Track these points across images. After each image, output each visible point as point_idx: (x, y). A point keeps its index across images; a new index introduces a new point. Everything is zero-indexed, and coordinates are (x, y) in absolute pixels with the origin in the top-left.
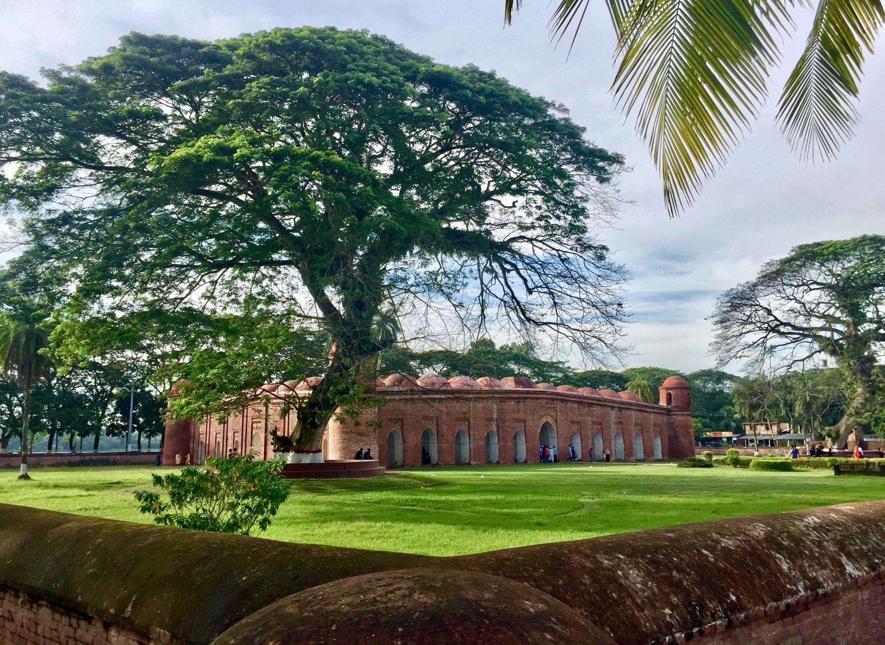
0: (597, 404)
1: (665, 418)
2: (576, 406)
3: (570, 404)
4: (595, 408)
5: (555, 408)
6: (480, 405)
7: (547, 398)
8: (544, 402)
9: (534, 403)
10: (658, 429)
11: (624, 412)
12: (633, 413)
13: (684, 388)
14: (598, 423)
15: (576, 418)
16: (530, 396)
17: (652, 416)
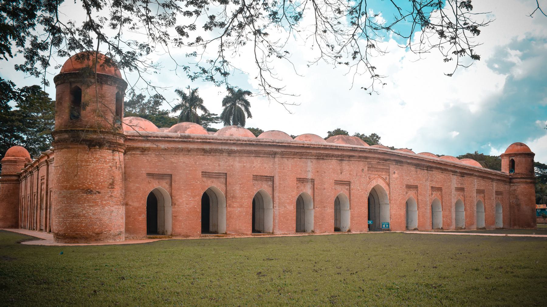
5: (388, 171)
7: (379, 159)
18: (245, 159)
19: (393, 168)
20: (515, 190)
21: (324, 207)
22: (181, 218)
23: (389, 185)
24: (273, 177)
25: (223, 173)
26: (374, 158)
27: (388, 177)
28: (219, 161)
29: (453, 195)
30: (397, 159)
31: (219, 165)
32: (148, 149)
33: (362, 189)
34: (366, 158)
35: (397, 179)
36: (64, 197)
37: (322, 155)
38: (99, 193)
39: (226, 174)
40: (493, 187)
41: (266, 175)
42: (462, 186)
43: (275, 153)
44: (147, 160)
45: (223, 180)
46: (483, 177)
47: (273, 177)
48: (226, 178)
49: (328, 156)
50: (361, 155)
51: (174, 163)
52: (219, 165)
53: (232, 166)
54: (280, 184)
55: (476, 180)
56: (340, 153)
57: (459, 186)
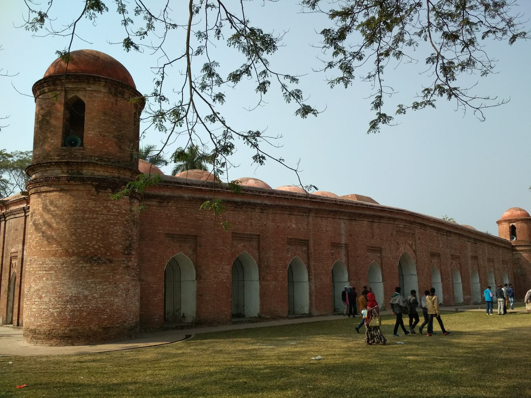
7: (406, 221)
21: (359, 279)
22: (207, 298)
23: (415, 252)
24: (308, 241)
25: (255, 235)
26: (402, 220)
27: (414, 242)
28: (251, 219)
31: (251, 225)
33: (392, 258)
36: (51, 269)
37: (355, 214)
38: (111, 261)
39: (259, 236)
41: (301, 238)
44: (167, 214)
45: (255, 244)
47: (308, 241)
48: (259, 242)
49: (360, 215)
51: (199, 220)
52: (251, 225)
53: (265, 225)
54: (315, 250)
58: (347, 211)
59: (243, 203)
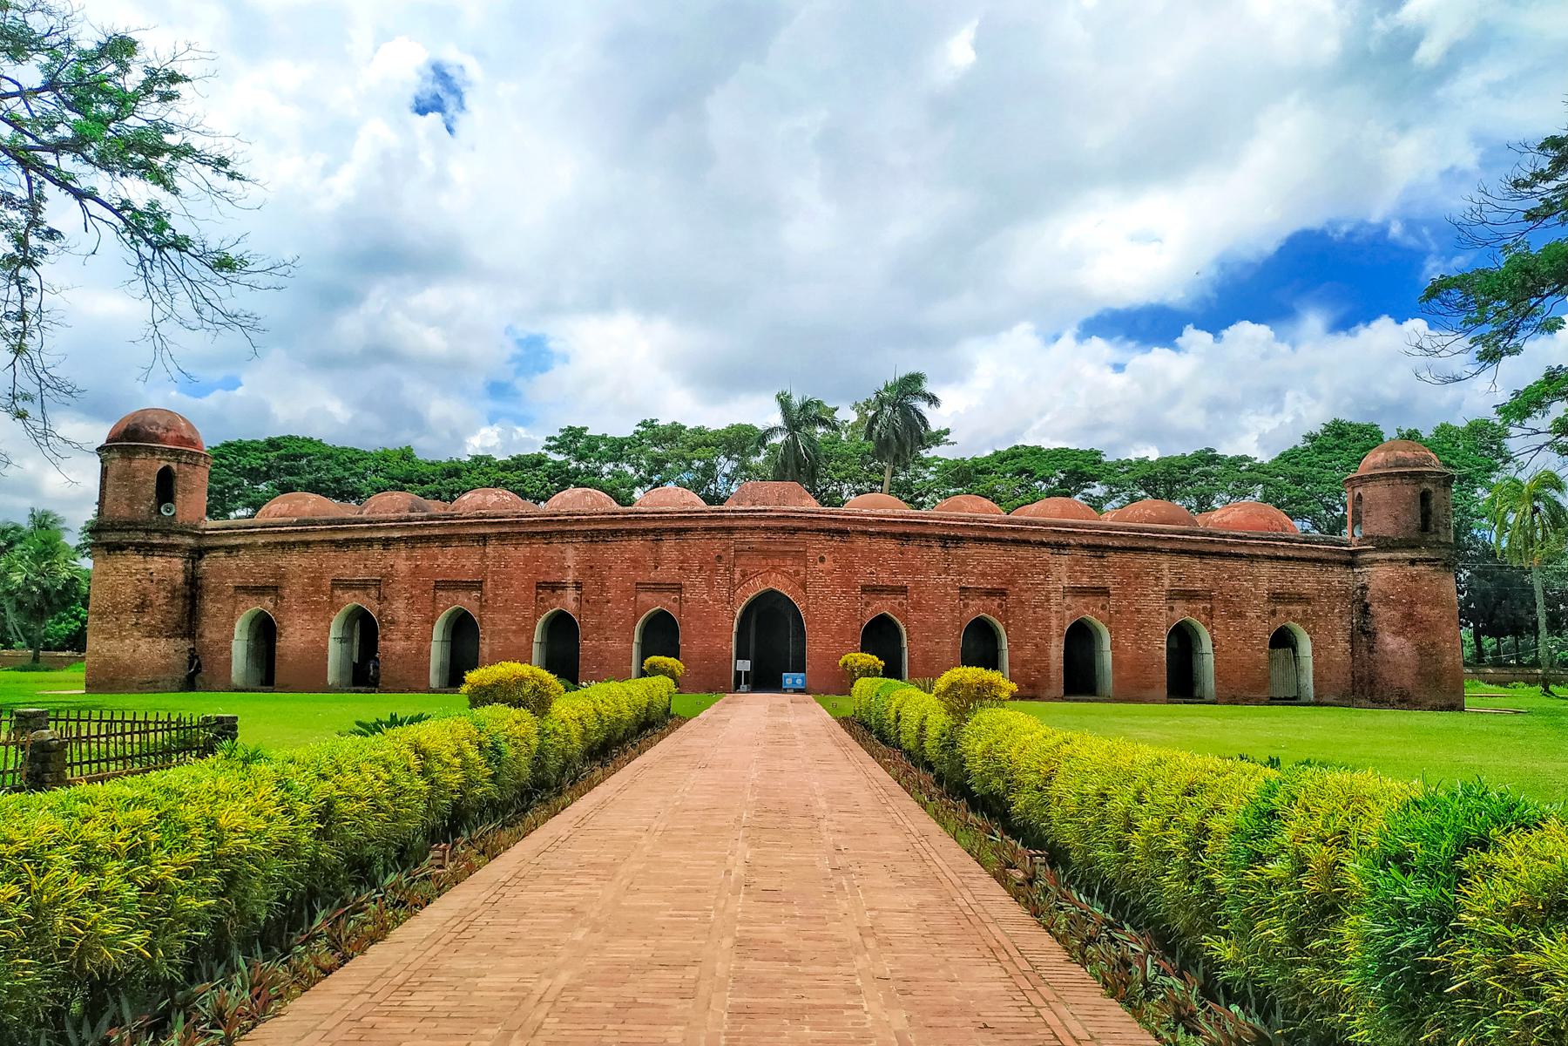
0: (976, 539)
1: (1337, 577)
2: (890, 545)
3: (861, 542)
4: (972, 549)
5: (801, 556)
6: (517, 553)
7: (767, 529)
8: (755, 539)
9: (717, 545)
10: (1298, 609)
11: (1114, 558)
12: (1165, 563)
13: (1402, 475)
14: (990, 593)
15: (884, 578)
16: (703, 524)
17: (1265, 569)
18: (418, 553)
19: (817, 545)
20: (1364, 587)
29: (1054, 608)
30: (833, 526)
32: (237, 547)
34: (729, 530)
35: (830, 573)
40: (1256, 579)
42: (1096, 583)
43: (484, 538)
46: (1201, 555)
49: (615, 532)
50: (714, 524)
55: (1165, 566)
56: (651, 525)
57: (1085, 581)
58: (586, 527)
59: (346, 540)
